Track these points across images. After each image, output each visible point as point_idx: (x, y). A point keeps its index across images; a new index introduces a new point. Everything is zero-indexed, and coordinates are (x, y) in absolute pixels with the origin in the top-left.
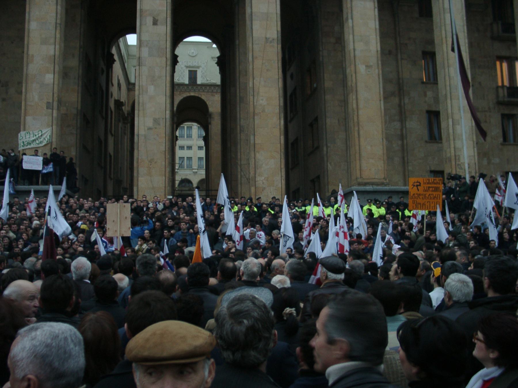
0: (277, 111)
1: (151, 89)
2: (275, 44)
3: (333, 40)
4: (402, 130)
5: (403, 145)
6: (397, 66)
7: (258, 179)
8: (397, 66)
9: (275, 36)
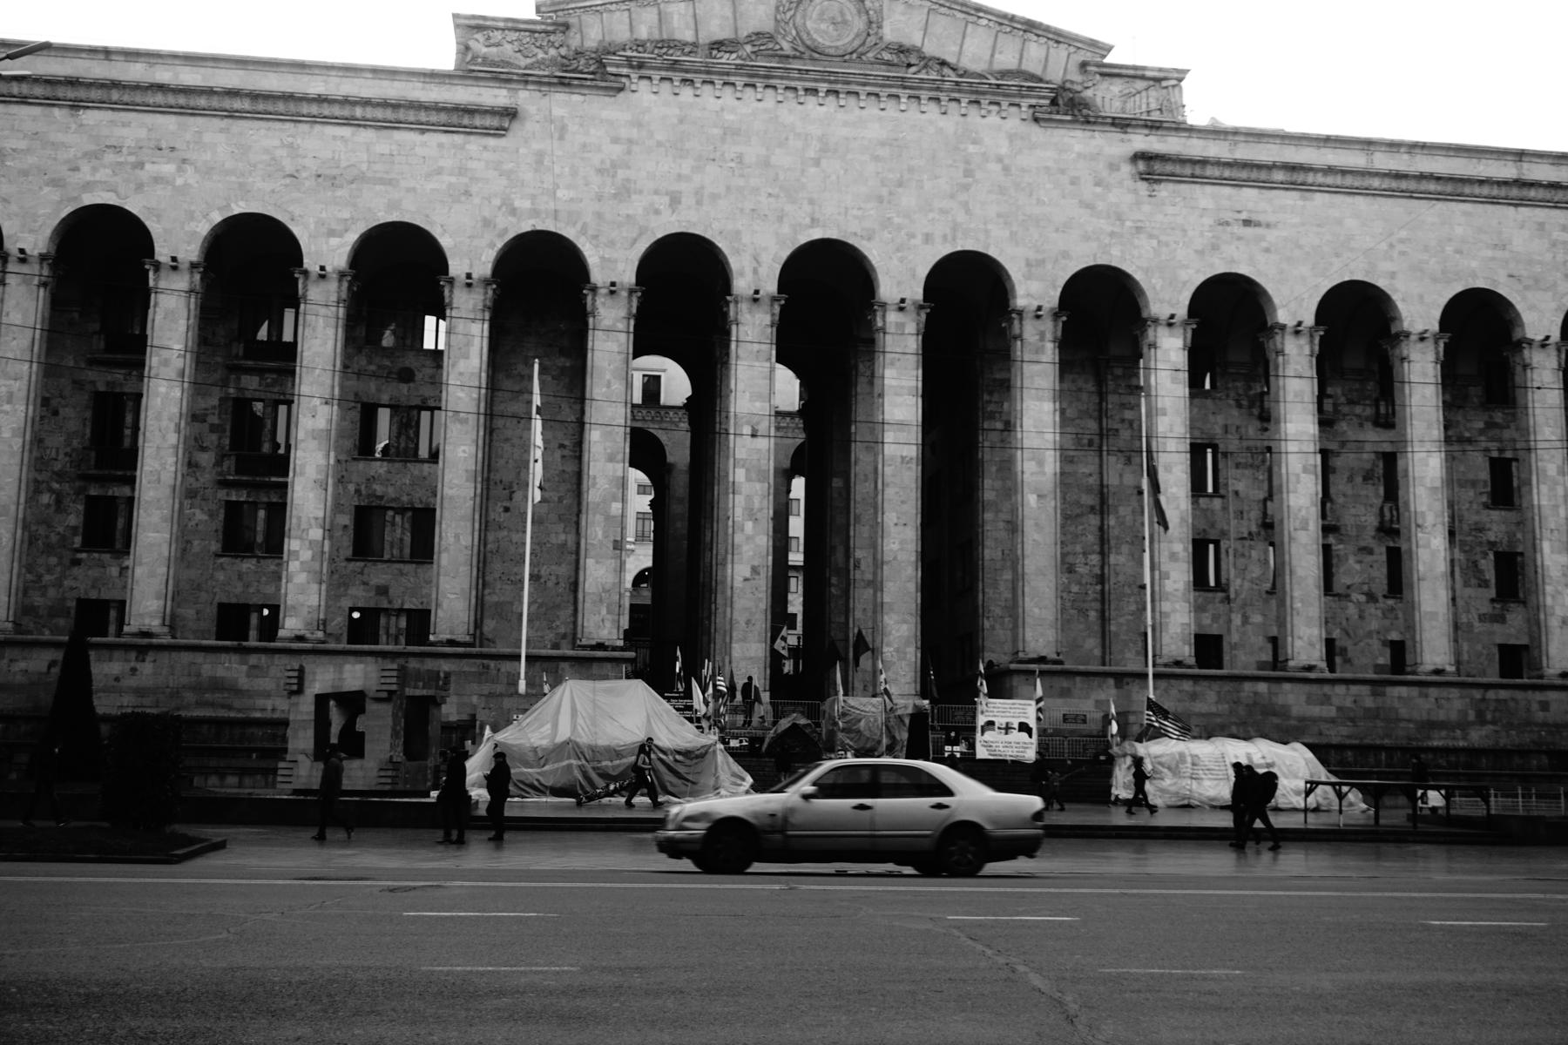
0: (913, 558)
1: (749, 526)
2: (914, 466)
3: (999, 425)
4: (1102, 568)
5: (1103, 591)
6: (1101, 466)
7: (885, 649)
8: (1101, 466)
9: (914, 454)
